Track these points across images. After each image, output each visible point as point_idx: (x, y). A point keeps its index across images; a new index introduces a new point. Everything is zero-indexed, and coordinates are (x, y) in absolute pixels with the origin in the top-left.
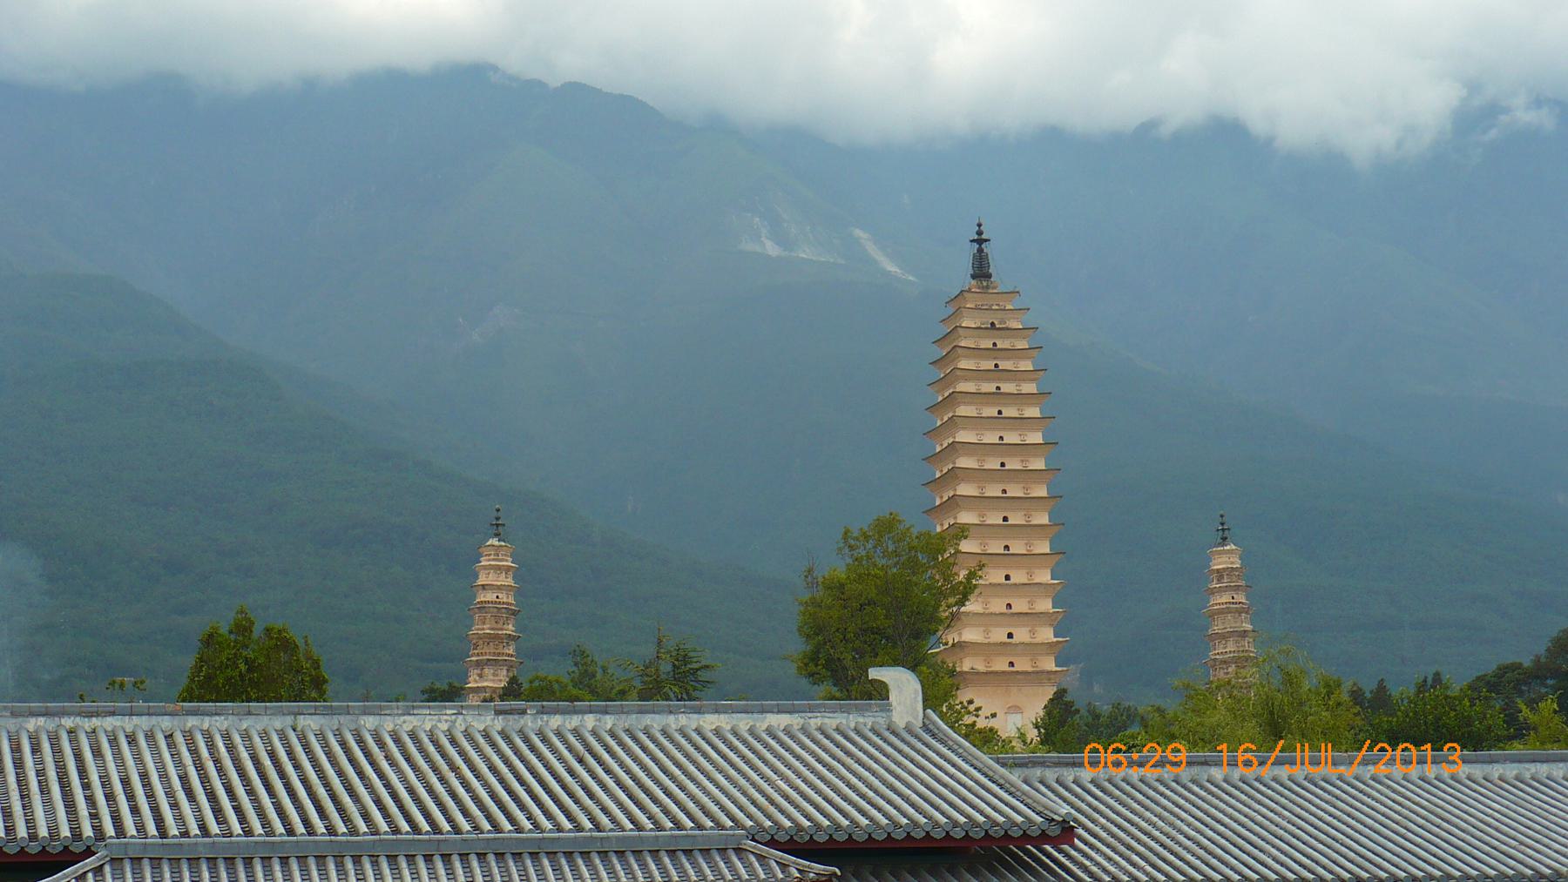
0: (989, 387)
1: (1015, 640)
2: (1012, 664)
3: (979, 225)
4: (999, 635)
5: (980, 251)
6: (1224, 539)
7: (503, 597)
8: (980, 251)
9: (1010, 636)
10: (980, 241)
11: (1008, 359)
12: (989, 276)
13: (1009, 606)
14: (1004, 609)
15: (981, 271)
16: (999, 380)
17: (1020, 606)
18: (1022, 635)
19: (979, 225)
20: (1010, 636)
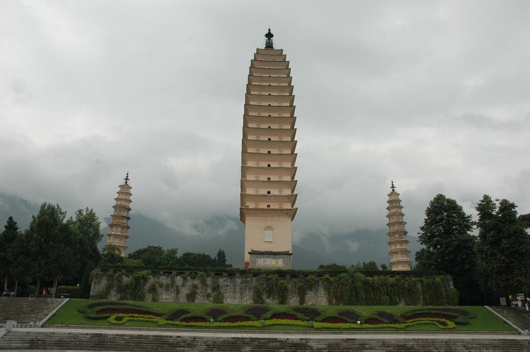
0: (268, 84)
1: (271, 194)
2: (269, 206)
3: (269, 30)
4: (264, 192)
5: (269, 39)
6: (393, 190)
7: (123, 203)
8: (269, 39)
9: (269, 192)
10: (269, 35)
11: (275, 74)
12: (272, 47)
13: (269, 178)
14: (267, 180)
15: (269, 46)
16: (270, 81)
17: (274, 178)
18: (275, 192)
19: (269, 30)
20: (269, 192)
